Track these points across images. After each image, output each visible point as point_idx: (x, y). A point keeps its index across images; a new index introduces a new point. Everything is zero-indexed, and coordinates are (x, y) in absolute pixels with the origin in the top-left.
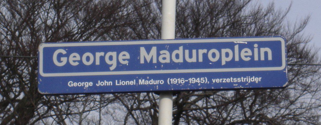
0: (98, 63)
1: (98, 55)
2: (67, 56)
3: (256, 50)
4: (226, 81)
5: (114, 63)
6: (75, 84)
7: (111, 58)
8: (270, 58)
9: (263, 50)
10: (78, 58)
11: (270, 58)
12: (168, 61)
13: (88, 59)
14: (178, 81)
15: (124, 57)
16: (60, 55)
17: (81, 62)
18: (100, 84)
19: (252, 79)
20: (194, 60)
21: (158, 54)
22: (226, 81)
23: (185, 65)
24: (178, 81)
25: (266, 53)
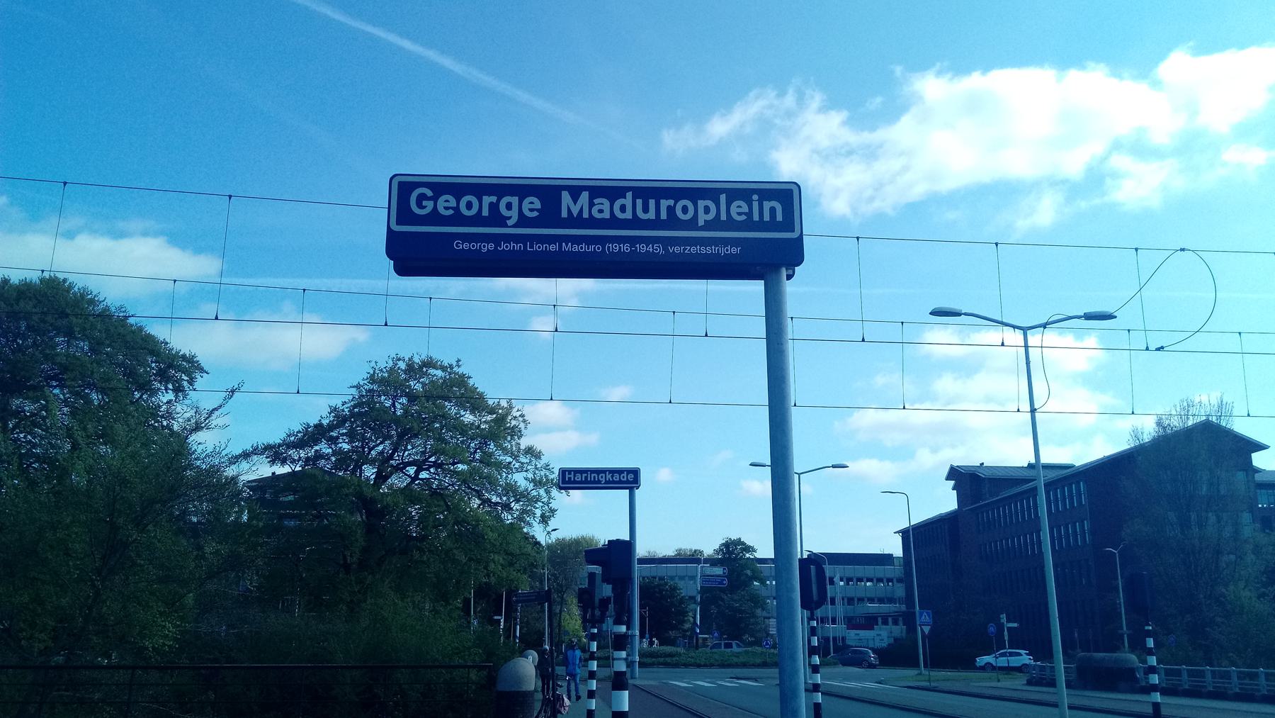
0: (485, 213)
1: (487, 200)
2: (435, 199)
3: (756, 205)
6: (466, 246)
7: (509, 206)
8: (779, 218)
9: (767, 205)
10: (453, 203)
11: (779, 218)
13: (469, 205)
15: (532, 205)
16: (422, 197)
17: (457, 209)
18: (503, 246)
20: (651, 215)
21: (591, 205)
23: (635, 223)
25: (773, 210)
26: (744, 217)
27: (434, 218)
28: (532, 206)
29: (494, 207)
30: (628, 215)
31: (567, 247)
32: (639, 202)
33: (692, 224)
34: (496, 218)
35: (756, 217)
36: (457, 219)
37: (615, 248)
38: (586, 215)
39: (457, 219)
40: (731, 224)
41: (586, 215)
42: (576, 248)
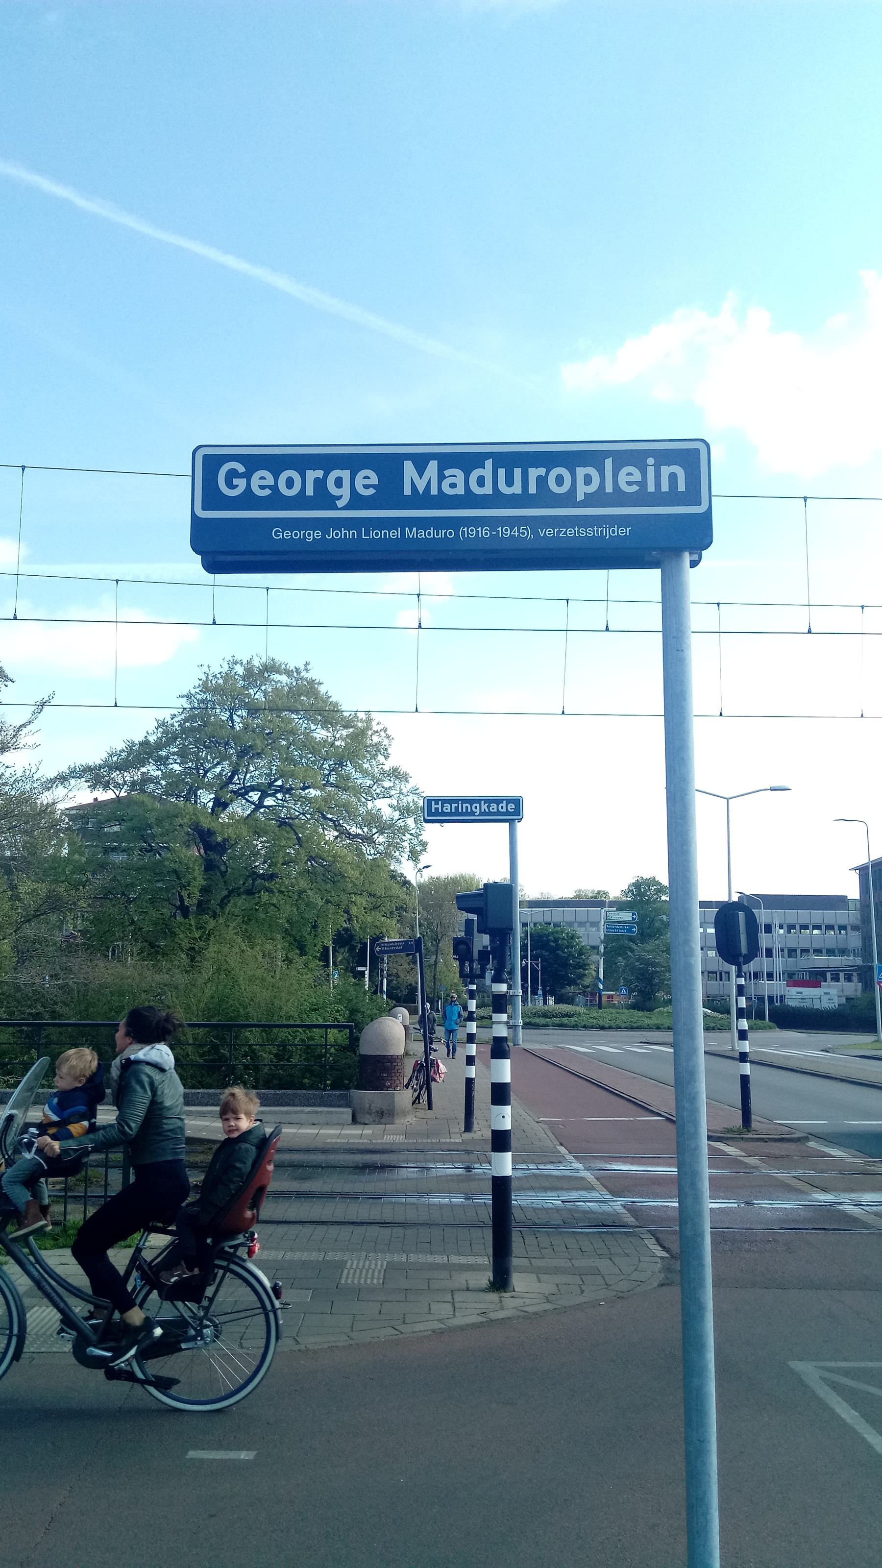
0: (310, 492)
1: (312, 475)
2: (248, 476)
3: (651, 471)
4: (565, 533)
5: (345, 493)
6: (287, 535)
7: (339, 483)
8: (681, 487)
9: (666, 471)
10: (270, 481)
11: (681, 487)
12: (460, 490)
13: (290, 483)
14: (477, 532)
16: (232, 475)
17: (275, 488)
18: (332, 534)
19: (613, 532)
20: (517, 489)
21: (441, 477)
22: (565, 533)
23: (497, 499)
24: (477, 532)
25: (673, 477)
26: (635, 488)
27: (248, 500)
28: (367, 482)
29: (320, 484)
30: (488, 489)
31: (411, 533)
32: (502, 472)
33: (568, 499)
34: (323, 498)
35: (651, 488)
36: (276, 500)
37: (471, 532)
38: (434, 491)
39: (276, 500)
40: (619, 498)
41: (434, 491)
42: (422, 534)
